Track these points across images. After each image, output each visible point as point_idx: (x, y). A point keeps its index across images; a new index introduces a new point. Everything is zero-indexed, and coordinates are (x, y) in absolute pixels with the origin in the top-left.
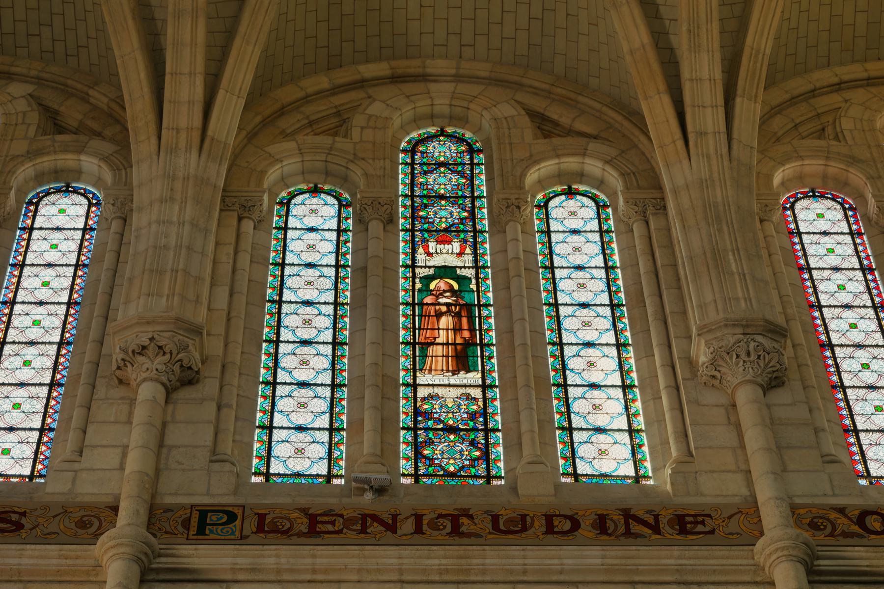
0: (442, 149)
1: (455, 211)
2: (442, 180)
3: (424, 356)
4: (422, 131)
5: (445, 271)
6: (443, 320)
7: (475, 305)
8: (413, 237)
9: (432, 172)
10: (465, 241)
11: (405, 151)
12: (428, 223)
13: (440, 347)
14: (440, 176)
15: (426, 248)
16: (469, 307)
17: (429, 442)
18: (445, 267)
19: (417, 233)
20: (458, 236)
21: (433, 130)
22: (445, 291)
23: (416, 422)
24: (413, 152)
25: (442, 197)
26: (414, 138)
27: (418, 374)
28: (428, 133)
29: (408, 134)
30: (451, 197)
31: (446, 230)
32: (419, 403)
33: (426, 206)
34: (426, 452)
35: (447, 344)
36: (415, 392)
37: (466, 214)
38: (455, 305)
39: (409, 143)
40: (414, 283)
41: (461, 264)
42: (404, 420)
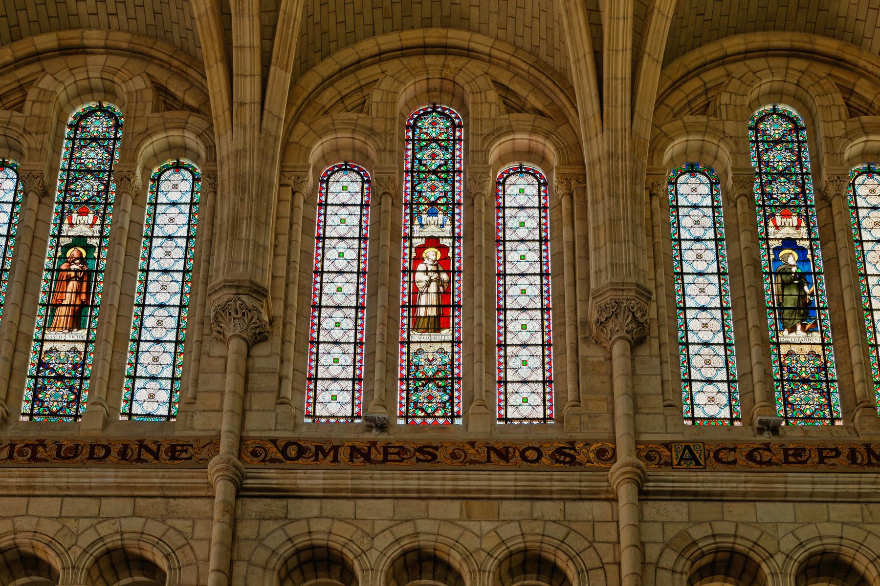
0: (97, 123)
1: (96, 183)
2: (92, 155)
3: (53, 316)
4: (85, 106)
5: (79, 241)
6: (71, 283)
7: (94, 271)
8: (63, 208)
9: (86, 147)
10: (98, 212)
11: (70, 126)
12: (76, 195)
13: (64, 308)
14: (91, 151)
15: (70, 219)
16: (89, 273)
17: (44, 388)
18: (80, 236)
19: (66, 205)
20: (94, 208)
21: (93, 105)
22: (76, 259)
23: (38, 371)
24: (75, 127)
25: (89, 171)
26: (79, 113)
27: (46, 332)
28: (90, 107)
29: (74, 108)
30: (95, 171)
31: (87, 202)
32: (43, 356)
33: (77, 179)
34: (40, 396)
35: (69, 305)
36: (42, 346)
37: (102, 187)
38: (81, 271)
39: (75, 118)
40: (57, 251)
41: (90, 234)
42: (31, 370)
